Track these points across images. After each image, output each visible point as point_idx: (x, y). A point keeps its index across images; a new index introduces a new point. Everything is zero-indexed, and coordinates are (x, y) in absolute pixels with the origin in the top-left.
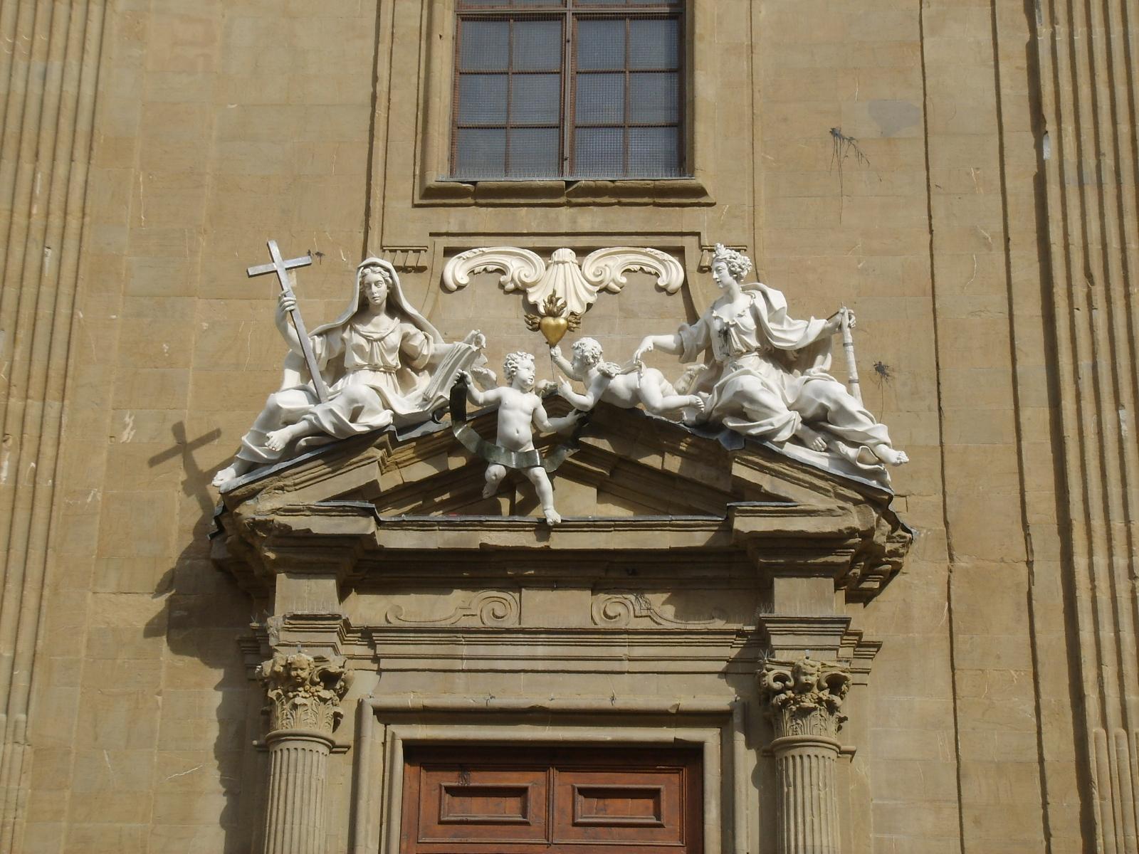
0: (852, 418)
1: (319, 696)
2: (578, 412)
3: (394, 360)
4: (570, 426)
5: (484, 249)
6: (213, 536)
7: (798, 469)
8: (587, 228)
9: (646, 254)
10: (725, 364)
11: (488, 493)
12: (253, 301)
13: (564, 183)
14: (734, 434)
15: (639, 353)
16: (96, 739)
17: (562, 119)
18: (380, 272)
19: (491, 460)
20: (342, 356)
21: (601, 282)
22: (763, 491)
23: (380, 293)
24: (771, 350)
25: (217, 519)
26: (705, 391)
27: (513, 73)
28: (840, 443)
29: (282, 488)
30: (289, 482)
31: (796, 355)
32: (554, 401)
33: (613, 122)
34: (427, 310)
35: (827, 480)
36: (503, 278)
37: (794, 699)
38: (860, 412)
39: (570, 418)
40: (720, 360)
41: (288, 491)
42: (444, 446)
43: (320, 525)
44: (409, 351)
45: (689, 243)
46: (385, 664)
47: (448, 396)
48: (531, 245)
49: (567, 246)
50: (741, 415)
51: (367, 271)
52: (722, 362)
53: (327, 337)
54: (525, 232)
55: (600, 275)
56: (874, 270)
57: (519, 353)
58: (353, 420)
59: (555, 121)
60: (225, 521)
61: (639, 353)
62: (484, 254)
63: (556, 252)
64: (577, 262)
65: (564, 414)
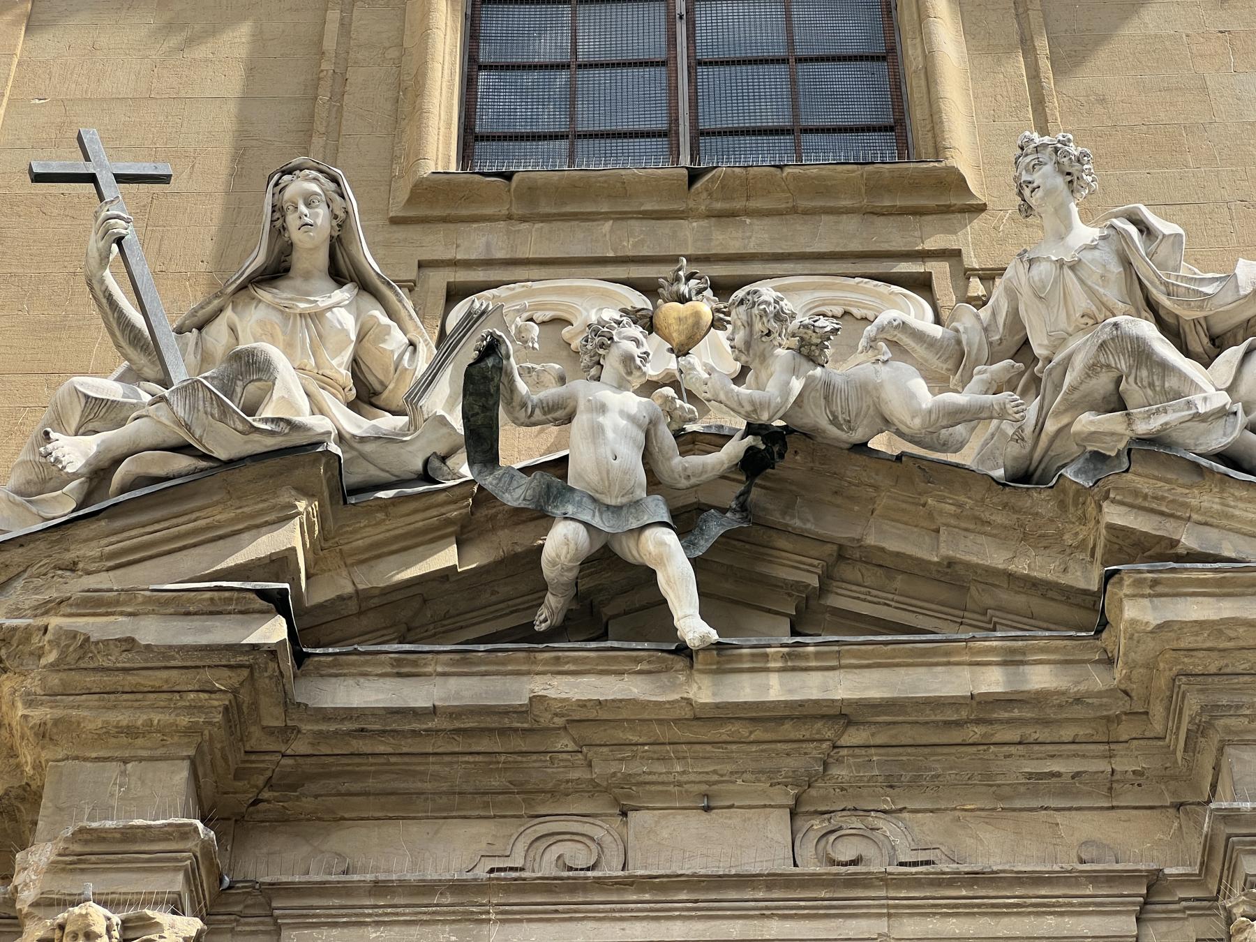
5: (529, 284)
8: (735, 247)
9: (854, 289)
11: (545, 620)
13: (685, 172)
18: (315, 179)
19: (558, 512)
22: (1181, 550)
23: (312, 226)
27: (579, 66)
29: (72, 567)
30: (93, 550)
33: (771, 123)
41: (89, 573)
42: (449, 522)
43: (152, 631)
44: (375, 372)
59: (662, 125)
62: (532, 293)
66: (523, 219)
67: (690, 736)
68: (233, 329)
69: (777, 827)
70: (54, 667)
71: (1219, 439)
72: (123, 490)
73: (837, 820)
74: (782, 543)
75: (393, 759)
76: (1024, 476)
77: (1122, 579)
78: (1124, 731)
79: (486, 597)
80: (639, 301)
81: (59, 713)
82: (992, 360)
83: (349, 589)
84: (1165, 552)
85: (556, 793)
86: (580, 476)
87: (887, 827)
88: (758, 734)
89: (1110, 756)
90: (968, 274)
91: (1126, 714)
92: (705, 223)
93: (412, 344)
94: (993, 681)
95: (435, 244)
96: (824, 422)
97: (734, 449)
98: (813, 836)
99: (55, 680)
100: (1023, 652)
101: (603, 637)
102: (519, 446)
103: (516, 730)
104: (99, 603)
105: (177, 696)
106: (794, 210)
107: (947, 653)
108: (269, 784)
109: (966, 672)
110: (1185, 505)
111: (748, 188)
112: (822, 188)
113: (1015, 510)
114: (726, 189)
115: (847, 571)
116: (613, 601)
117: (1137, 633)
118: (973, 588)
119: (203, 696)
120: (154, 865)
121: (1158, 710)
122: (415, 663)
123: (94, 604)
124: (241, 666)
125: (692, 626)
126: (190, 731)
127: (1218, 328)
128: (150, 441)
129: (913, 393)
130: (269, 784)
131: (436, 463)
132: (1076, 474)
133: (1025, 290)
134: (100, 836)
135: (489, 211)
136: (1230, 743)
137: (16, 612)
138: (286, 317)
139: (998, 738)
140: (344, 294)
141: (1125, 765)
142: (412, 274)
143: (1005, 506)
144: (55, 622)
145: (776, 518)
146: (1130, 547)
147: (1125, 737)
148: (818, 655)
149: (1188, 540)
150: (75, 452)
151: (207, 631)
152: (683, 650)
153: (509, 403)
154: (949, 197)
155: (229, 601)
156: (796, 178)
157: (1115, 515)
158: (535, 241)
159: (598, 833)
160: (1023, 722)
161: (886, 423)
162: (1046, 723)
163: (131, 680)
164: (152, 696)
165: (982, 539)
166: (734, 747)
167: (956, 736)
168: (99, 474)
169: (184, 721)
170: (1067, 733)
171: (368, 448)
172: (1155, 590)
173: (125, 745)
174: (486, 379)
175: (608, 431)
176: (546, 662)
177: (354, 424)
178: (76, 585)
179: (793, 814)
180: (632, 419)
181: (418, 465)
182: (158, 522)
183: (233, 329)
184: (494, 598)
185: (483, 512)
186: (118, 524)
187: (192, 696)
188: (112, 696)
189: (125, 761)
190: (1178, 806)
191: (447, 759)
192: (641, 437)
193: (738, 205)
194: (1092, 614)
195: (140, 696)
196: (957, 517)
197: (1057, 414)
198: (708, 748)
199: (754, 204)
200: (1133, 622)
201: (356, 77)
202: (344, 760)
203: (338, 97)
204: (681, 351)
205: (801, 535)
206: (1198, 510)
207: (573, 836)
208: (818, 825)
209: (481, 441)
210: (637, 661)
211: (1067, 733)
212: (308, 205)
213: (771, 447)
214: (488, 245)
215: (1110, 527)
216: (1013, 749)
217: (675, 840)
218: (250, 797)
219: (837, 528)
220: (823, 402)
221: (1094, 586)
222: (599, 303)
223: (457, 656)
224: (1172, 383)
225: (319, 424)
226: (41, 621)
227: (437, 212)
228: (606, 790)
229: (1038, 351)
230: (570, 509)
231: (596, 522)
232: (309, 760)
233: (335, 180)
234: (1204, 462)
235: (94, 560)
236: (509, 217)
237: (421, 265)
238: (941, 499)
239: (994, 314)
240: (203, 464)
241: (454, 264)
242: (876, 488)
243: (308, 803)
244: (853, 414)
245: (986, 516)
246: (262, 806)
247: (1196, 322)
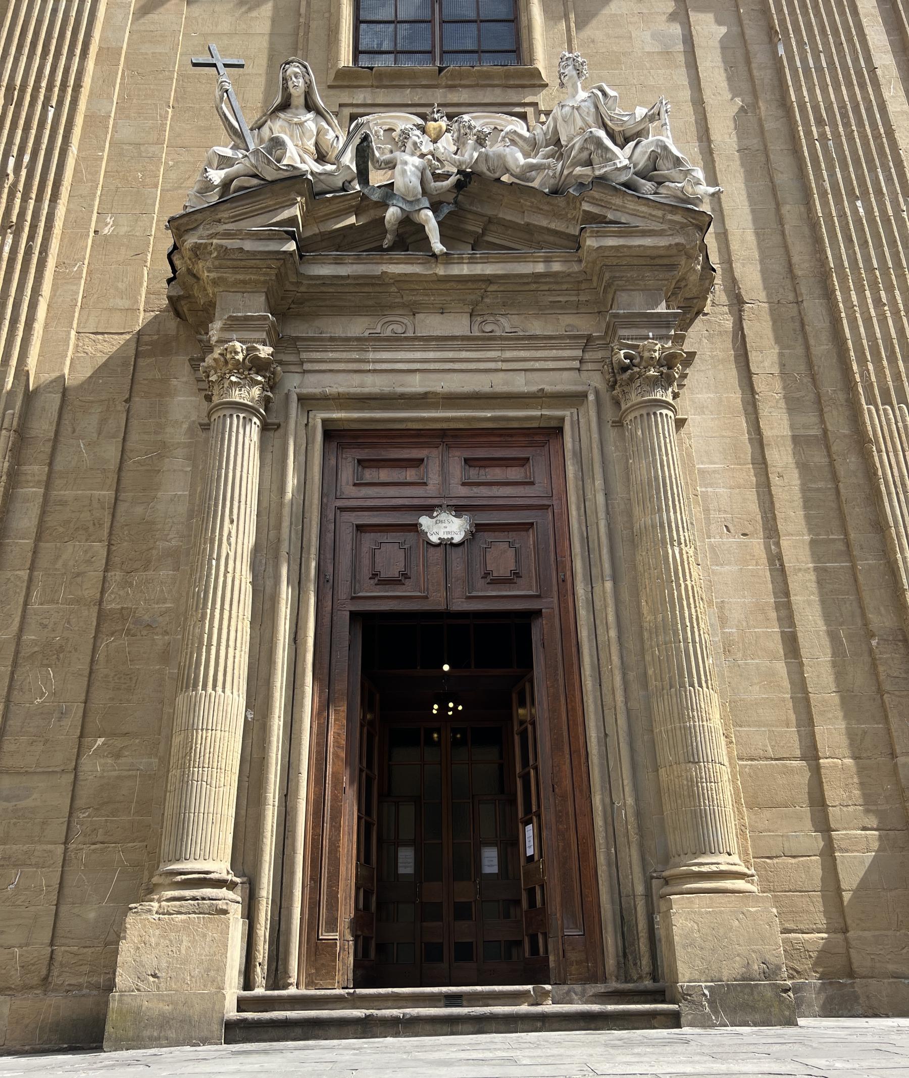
1: (252, 379)
3: (310, 145)
7: (637, 202)
9: (499, 118)
16: (74, 432)
17: (434, 46)
23: (298, 86)
29: (219, 221)
30: (225, 215)
33: (470, 48)
35: (659, 209)
36: (394, 134)
37: (638, 373)
42: (353, 206)
43: (248, 246)
44: (324, 147)
45: (530, 111)
46: (307, 366)
48: (414, 112)
59: (429, 48)
62: (381, 118)
66: (377, 87)
67: (436, 287)
68: (271, 129)
69: (466, 320)
71: (624, 178)
72: (234, 192)
74: (469, 216)
76: (555, 192)
78: (583, 286)
80: (420, 121)
81: (219, 275)
82: (546, 147)
83: (317, 231)
84: (601, 220)
85: (391, 307)
86: (398, 190)
87: (502, 320)
89: (578, 295)
90: (540, 112)
92: (444, 90)
93: (337, 137)
94: (540, 268)
95: (345, 97)
96: (485, 170)
97: (452, 180)
98: (478, 323)
99: (217, 263)
100: (551, 257)
101: (407, 250)
102: (377, 178)
104: (230, 235)
106: (477, 85)
107: (525, 258)
109: (531, 264)
110: (610, 203)
111: (460, 75)
112: (487, 76)
113: (552, 205)
114: (453, 75)
115: (493, 227)
117: (591, 250)
120: (256, 329)
121: (595, 279)
122: (341, 259)
123: (228, 235)
125: (438, 246)
126: (265, 282)
127: (628, 134)
128: (243, 173)
129: (518, 158)
131: (347, 184)
133: (560, 118)
134: (236, 319)
135: (365, 83)
136: (618, 290)
137: (201, 238)
138: (290, 124)
140: (311, 115)
141: (583, 298)
142: (336, 109)
143: (548, 203)
144: (215, 241)
145: (467, 207)
146: (591, 218)
148: (481, 258)
149: (610, 216)
150: (217, 176)
151: (268, 246)
152: (434, 255)
153: (372, 160)
154: (534, 81)
155: (275, 235)
156: (478, 71)
157: (586, 207)
158: (382, 97)
159: (406, 321)
160: (550, 283)
161: (507, 170)
162: (557, 283)
165: (539, 216)
167: (527, 288)
168: (226, 184)
169: (262, 278)
170: (565, 287)
171: (322, 177)
172: (598, 235)
173: (243, 287)
174: (364, 151)
175: (408, 171)
176: (387, 259)
177: (318, 168)
178: (222, 228)
179: (471, 315)
180: (417, 167)
181: (341, 185)
183: (271, 129)
185: (365, 203)
186: (234, 205)
189: (243, 293)
190: (599, 313)
192: (420, 174)
193: (457, 82)
194: (576, 243)
196: (531, 207)
197: (568, 167)
199: (463, 82)
200: (589, 246)
201: (313, 25)
203: (307, 33)
204: (435, 141)
205: (476, 213)
206: (614, 205)
207: (397, 322)
208: (479, 319)
209: (363, 175)
210: (419, 259)
211: (565, 287)
212: (296, 77)
213: (467, 179)
214: (365, 98)
215: (584, 211)
217: (432, 324)
218: (287, 307)
219: (489, 211)
221: (577, 234)
222: (405, 121)
224: (609, 155)
225: (304, 167)
226: (210, 241)
227: (345, 84)
228: (408, 306)
229: (563, 143)
230: (395, 202)
231: (404, 207)
233: (305, 67)
234: (618, 186)
235: (226, 218)
236: (372, 86)
237: (340, 105)
238: (526, 200)
239: (548, 128)
240: (263, 182)
241: (352, 105)
245: (541, 207)
247: (620, 132)
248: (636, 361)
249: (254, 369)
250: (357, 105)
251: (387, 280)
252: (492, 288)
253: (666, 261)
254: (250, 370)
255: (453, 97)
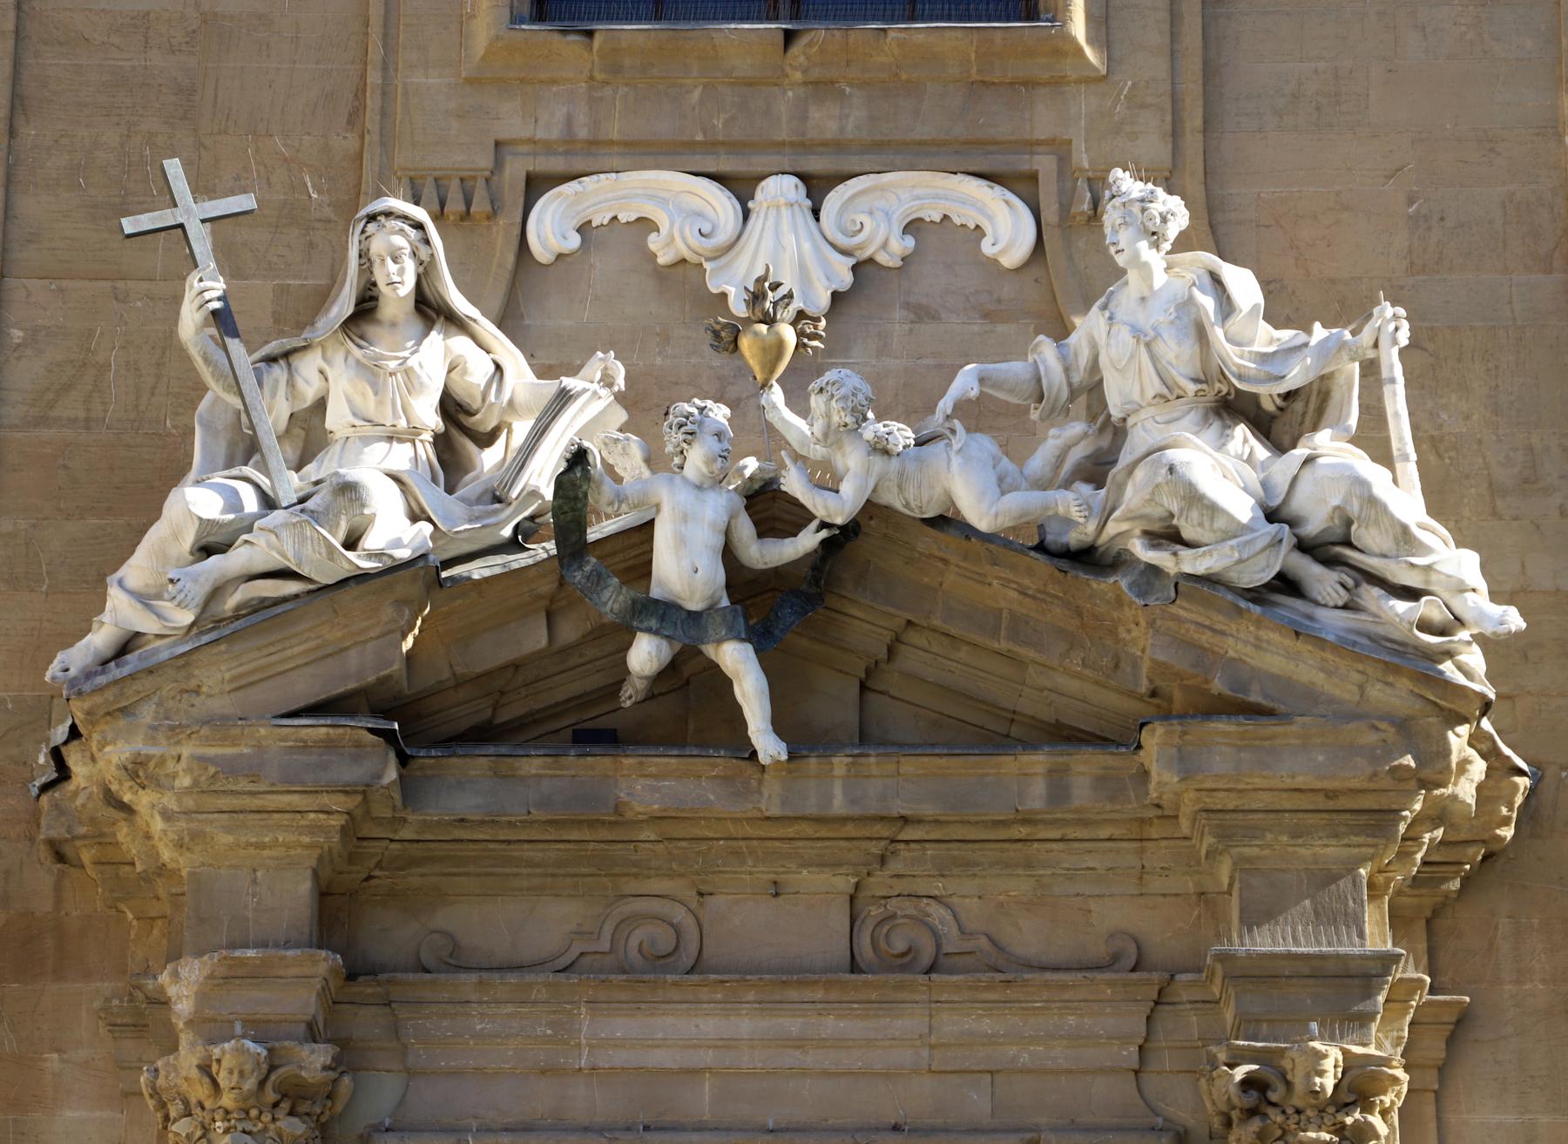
0: (1405, 537)
2: (824, 525)
4: (808, 555)
6: (45, 788)
8: (831, 129)
10: (1130, 422)
12: (120, 284)
14: (1154, 570)
15: (945, 405)
20: (321, 405)
21: (861, 247)
24: (1228, 394)
25: (56, 754)
26: (1088, 480)
28: (1376, 591)
31: (1279, 401)
32: (769, 507)
34: (496, 302)
38: (1420, 526)
39: (808, 540)
40: (1121, 415)
42: (540, 597)
47: (549, 494)
48: (712, 169)
49: (787, 169)
50: (1169, 536)
51: (371, 227)
52: (1124, 420)
53: (289, 365)
54: (699, 137)
55: (860, 230)
56: (1442, 219)
57: (696, 401)
58: (351, 544)
60: (74, 758)
61: (945, 405)
63: (763, 183)
64: (809, 203)
65: (793, 530)
70: (188, 791)
73: (893, 905)
75: (491, 846)
77: (1154, 730)
79: (573, 661)
88: (823, 833)
91: (1159, 817)
93: (498, 367)
96: (898, 505)
99: (190, 803)
103: (603, 822)
105: (298, 816)
108: (379, 865)
115: (914, 637)
116: (693, 696)
118: (1031, 669)
119: (322, 816)
124: (355, 792)
125: (768, 745)
130: (379, 865)
131: (528, 524)
132: (1130, 587)
134: (242, 962)
139: (1041, 835)
147: (1155, 836)
160: (1064, 823)
162: (1085, 823)
163: (257, 803)
164: (276, 816)
166: (800, 844)
169: (306, 839)
182: (272, 644)
183: (321, 372)
184: (582, 660)
187: (312, 816)
188: (241, 816)
191: (540, 846)
195: (265, 816)
198: (777, 844)
202: (447, 846)
211: (1104, 833)
214: (569, 120)
216: (1054, 846)
220: (896, 490)
223: (549, 760)
232: (416, 845)
237: (498, 144)
242: (945, 562)
243: (415, 881)
244: (925, 501)
246: (373, 882)
248: (1273, 1097)
249: (285, 1105)
250: (548, 147)
251: (629, 815)
252: (910, 833)
253: (1368, 802)
254: (276, 1105)
255: (825, 121)
